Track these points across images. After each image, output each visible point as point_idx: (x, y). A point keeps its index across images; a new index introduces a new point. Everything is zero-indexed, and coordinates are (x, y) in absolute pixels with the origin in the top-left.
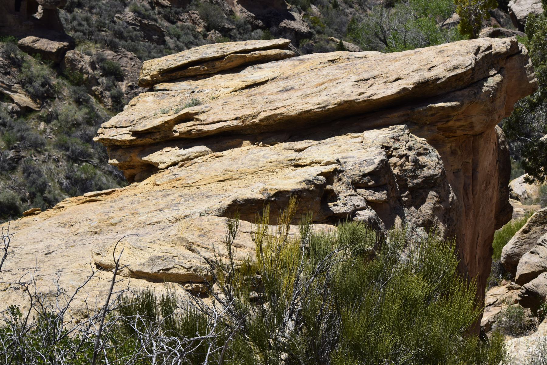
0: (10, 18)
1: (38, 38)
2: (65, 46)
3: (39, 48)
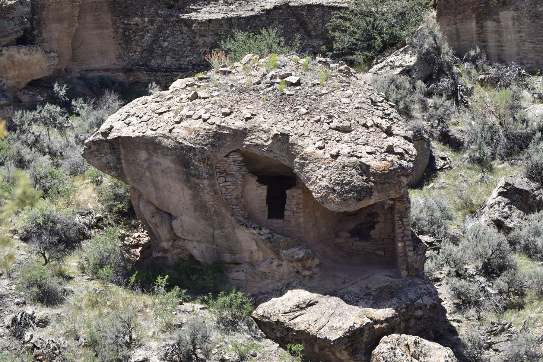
0: (247, 240)
1: (314, 296)
2: (376, 322)
3: (303, 327)
